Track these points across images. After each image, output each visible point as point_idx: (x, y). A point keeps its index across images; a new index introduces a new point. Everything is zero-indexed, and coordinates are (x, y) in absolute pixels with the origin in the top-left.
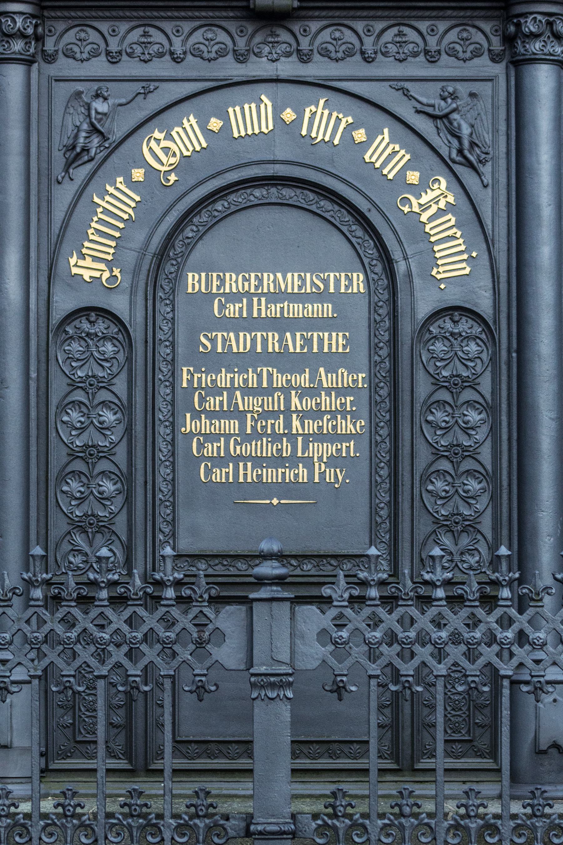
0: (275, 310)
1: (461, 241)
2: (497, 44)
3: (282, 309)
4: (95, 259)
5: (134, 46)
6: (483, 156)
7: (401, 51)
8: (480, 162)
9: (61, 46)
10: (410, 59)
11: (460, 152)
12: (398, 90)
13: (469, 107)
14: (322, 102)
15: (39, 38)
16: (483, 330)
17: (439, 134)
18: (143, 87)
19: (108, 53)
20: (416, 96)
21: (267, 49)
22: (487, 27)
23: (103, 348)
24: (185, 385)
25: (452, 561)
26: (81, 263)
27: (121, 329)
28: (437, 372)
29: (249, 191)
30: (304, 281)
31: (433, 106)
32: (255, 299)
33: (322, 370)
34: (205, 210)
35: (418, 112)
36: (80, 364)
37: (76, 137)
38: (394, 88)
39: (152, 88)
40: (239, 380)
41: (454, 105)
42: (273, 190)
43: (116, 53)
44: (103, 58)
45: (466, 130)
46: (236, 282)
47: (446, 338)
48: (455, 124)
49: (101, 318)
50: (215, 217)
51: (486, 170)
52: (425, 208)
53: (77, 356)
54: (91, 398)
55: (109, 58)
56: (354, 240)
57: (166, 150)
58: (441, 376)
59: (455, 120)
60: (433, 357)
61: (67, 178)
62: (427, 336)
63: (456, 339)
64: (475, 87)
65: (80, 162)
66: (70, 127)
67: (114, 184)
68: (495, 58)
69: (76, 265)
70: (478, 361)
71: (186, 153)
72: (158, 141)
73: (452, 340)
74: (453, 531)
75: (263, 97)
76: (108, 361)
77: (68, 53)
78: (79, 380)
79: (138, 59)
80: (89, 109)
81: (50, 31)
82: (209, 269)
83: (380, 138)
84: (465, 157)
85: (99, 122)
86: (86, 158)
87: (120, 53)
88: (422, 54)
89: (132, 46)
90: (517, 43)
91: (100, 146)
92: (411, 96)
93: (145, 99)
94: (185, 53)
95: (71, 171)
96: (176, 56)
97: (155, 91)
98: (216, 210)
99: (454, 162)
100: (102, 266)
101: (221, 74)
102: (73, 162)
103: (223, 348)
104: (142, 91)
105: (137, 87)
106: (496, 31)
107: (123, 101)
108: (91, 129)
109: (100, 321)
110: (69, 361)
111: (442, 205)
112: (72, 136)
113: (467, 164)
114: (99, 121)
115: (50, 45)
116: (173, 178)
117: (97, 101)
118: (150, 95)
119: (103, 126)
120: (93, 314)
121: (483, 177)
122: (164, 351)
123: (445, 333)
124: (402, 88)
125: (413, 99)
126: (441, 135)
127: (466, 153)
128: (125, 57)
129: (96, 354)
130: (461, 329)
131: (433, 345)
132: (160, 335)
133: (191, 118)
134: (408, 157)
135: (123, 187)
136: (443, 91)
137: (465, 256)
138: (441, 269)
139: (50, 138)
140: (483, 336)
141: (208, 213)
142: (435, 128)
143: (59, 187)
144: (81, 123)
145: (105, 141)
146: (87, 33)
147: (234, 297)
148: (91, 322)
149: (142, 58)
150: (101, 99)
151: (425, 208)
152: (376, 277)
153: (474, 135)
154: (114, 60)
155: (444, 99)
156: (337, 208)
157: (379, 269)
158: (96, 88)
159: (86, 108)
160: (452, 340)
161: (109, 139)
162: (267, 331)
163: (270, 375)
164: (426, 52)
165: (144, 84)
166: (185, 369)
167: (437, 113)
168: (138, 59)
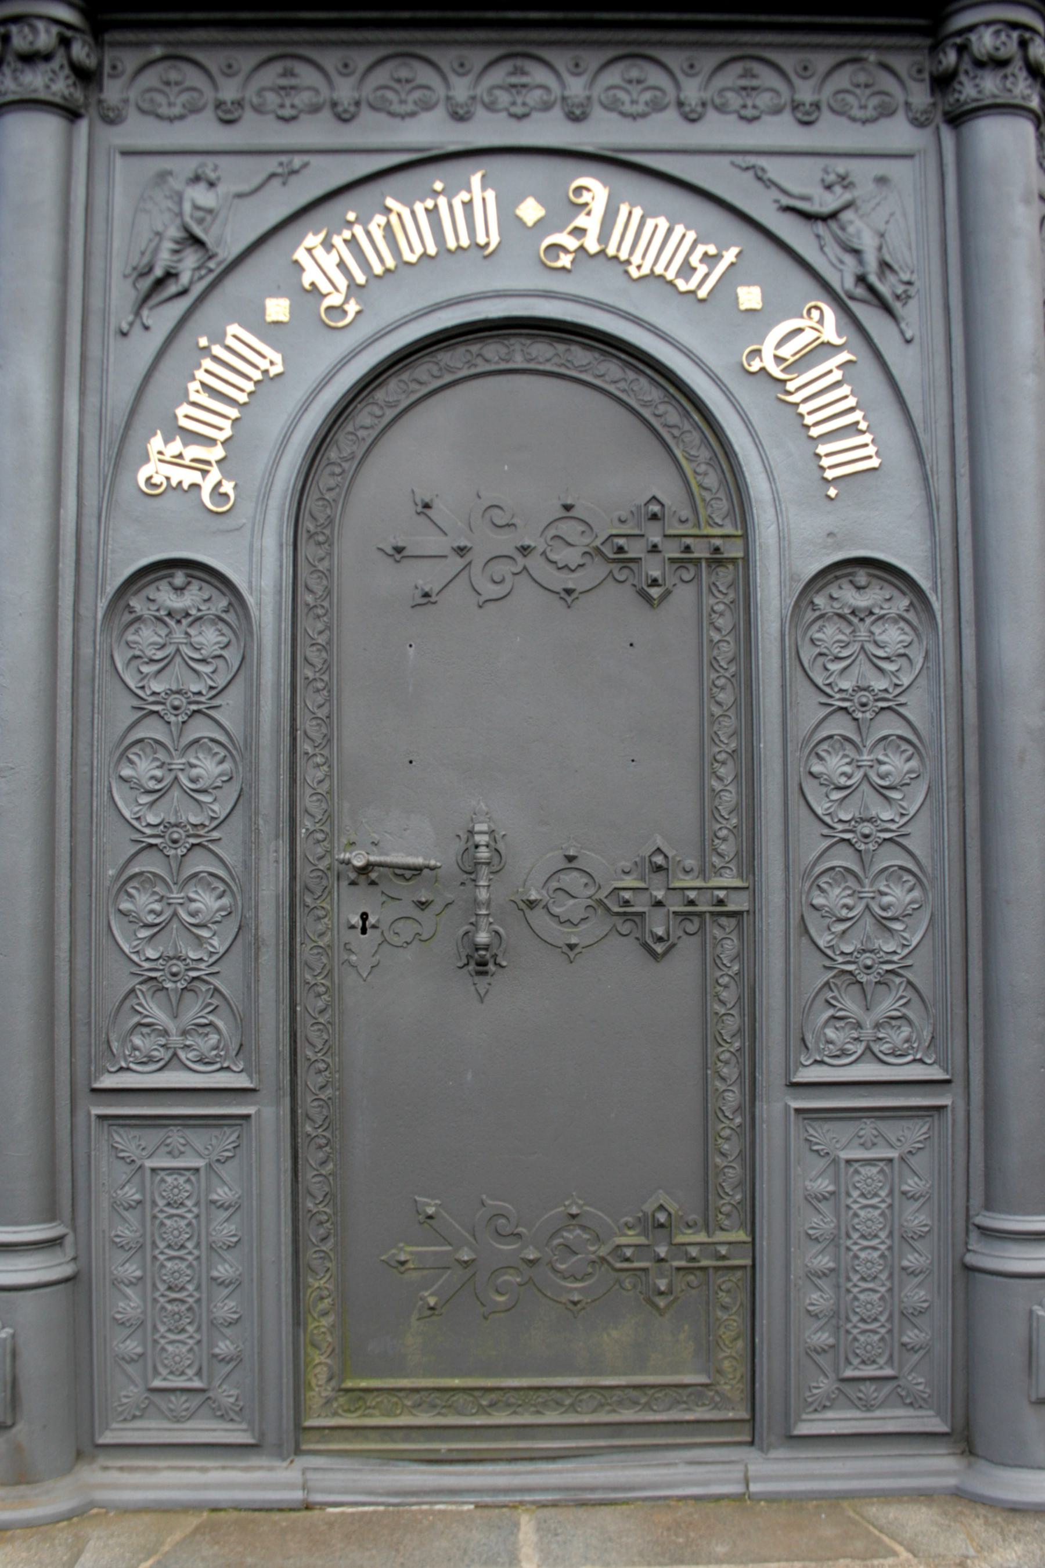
1: (867, 438)
2: (921, 96)
7: (749, 103)
8: (898, 297)
11: (861, 279)
12: (747, 169)
13: (877, 200)
16: (912, 604)
17: (822, 248)
19: (219, 105)
22: (901, 63)
23: (200, 639)
25: (857, 1039)
36: (156, 667)
37: (156, 251)
41: (847, 196)
44: (209, 113)
48: (851, 229)
51: (909, 312)
53: (150, 652)
54: (175, 733)
58: (836, 689)
59: (851, 222)
60: (821, 654)
61: (137, 329)
63: (862, 620)
70: (903, 661)
73: (855, 620)
74: (861, 983)
76: (208, 663)
77: (146, 106)
78: (151, 699)
80: (180, 202)
84: (871, 289)
87: (239, 104)
88: (788, 109)
91: (199, 268)
92: (770, 180)
94: (357, 104)
95: (145, 313)
99: (852, 298)
102: (147, 297)
104: (280, 170)
105: (271, 164)
106: (920, 71)
107: (245, 188)
109: (195, 585)
113: (875, 301)
114: (200, 221)
118: (293, 179)
119: (206, 231)
121: (903, 326)
126: (826, 249)
127: (873, 279)
128: (249, 115)
129: (186, 650)
140: (911, 616)
143: (126, 342)
144: (166, 226)
145: (210, 258)
153: (884, 250)
155: (829, 187)
164: (796, 106)
165: (284, 159)
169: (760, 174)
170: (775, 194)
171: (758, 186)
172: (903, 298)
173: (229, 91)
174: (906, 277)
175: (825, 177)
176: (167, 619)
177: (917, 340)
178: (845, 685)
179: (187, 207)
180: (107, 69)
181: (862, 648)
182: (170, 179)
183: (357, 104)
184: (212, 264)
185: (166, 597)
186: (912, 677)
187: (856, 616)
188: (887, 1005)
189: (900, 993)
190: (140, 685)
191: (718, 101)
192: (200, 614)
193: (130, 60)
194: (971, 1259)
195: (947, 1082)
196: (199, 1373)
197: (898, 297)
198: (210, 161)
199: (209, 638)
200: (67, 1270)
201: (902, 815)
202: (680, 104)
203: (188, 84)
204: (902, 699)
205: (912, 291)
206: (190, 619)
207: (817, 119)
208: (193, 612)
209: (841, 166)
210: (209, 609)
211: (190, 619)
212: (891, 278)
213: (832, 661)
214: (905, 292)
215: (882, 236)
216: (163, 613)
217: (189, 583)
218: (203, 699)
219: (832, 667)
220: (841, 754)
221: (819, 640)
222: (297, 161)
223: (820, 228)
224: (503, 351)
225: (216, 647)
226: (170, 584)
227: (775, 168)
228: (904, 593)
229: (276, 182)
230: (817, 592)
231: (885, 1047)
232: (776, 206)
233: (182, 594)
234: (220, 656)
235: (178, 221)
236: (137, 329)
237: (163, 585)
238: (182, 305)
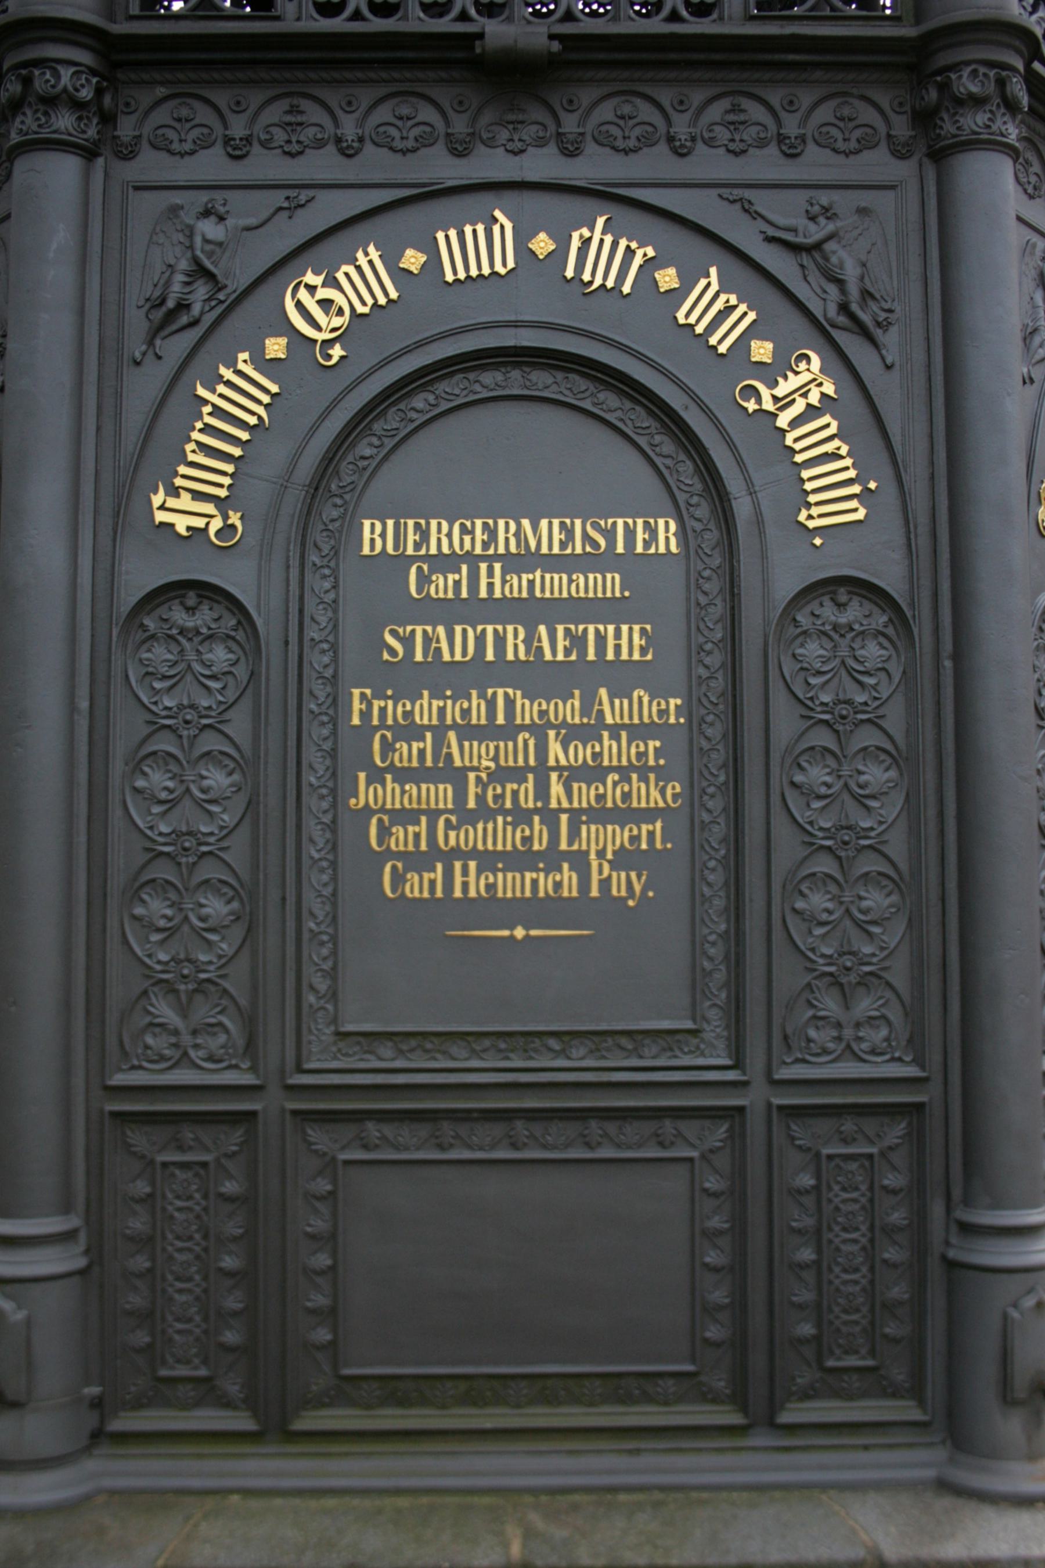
0: (518, 585)
1: (848, 462)
2: (902, 128)
3: (531, 583)
4: (197, 496)
5: (275, 130)
6: (884, 315)
7: (737, 137)
8: (879, 324)
9: (147, 130)
10: (752, 150)
11: (844, 308)
12: (734, 201)
13: (859, 231)
14: (600, 222)
15: (108, 119)
16: (890, 620)
18: (288, 198)
19: (228, 141)
20: (764, 212)
21: (504, 135)
23: (210, 656)
24: (356, 721)
26: (172, 503)
27: (242, 620)
28: (809, 695)
29: (472, 376)
30: (570, 533)
31: (794, 230)
32: (483, 566)
33: (603, 692)
34: (394, 409)
35: (771, 240)
37: (168, 284)
38: (727, 199)
39: (303, 198)
40: (453, 712)
41: (831, 227)
42: (516, 374)
43: (241, 139)
44: (218, 149)
45: (851, 273)
46: (449, 535)
47: (825, 633)
48: (834, 260)
49: (205, 601)
50: (412, 421)
51: (890, 339)
52: (784, 403)
53: (164, 670)
55: (229, 149)
56: (658, 461)
57: (325, 304)
58: (817, 703)
59: (834, 252)
60: (802, 669)
61: (150, 355)
62: (792, 631)
63: (842, 636)
64: (865, 198)
65: (174, 327)
66: (159, 267)
67: (232, 364)
68: (900, 153)
69: (162, 507)
70: (883, 675)
71: (361, 309)
72: (312, 289)
73: (836, 637)
75: (497, 214)
79: (279, 151)
80: (191, 236)
81: (127, 105)
82: (399, 514)
83: (703, 282)
85: (209, 258)
86: (184, 320)
87: (248, 140)
88: (774, 143)
89: (271, 129)
90: (942, 119)
91: (209, 299)
92: (756, 212)
93: (290, 217)
94: (361, 140)
95: (158, 342)
96: (345, 145)
97: (309, 205)
98: (413, 409)
99: (834, 326)
100: (209, 508)
101: (423, 177)
102: (162, 326)
103: (425, 654)
104: (286, 205)
105: (278, 198)
106: (901, 104)
107: (253, 221)
108: (194, 268)
111: (814, 398)
112: (162, 282)
113: (856, 329)
114: (210, 255)
115: (126, 129)
116: (337, 352)
117: (206, 221)
118: (300, 212)
120: (192, 594)
121: (884, 352)
122: (318, 660)
123: (823, 624)
124: (741, 199)
125: (759, 219)
126: (809, 278)
127: (854, 307)
128: (256, 149)
130: (851, 618)
131: (802, 645)
132: (312, 633)
133: (371, 249)
134: (752, 316)
135: (248, 370)
136: (812, 205)
137: (856, 489)
138: (815, 511)
139: (122, 288)
140: (890, 631)
141: (399, 413)
142: (798, 267)
145: (220, 290)
146: (192, 108)
147: (445, 563)
148: (188, 609)
149: (286, 149)
150: (213, 219)
151: (784, 403)
152: (698, 526)
154: (238, 153)
155: (813, 219)
156: (628, 405)
157: (703, 511)
158: (205, 199)
159: (188, 233)
160: (836, 637)
161: (226, 286)
162: (504, 623)
163: (510, 703)
164: (781, 139)
165: (292, 193)
166: (356, 692)
167: (800, 240)
168: (279, 151)
169: (747, 207)
171: (745, 217)
173: (238, 129)
175: (809, 208)
176: (180, 638)
177: (897, 367)
178: (826, 698)
179: (198, 240)
180: (121, 107)
181: (843, 662)
182: (182, 213)
183: (361, 140)
184: (221, 296)
185: (179, 616)
186: (890, 692)
187: (836, 632)
188: (865, 1005)
189: (879, 994)
191: (706, 135)
193: (145, 98)
194: (952, 1254)
195: (926, 1080)
196: (205, 1362)
197: (879, 324)
198: (218, 195)
199: (220, 655)
201: (881, 823)
202: (670, 139)
203: (197, 121)
204: (880, 712)
205: (893, 317)
207: (802, 151)
209: (824, 198)
212: (873, 306)
213: (814, 675)
214: (886, 319)
215: (864, 265)
217: (200, 603)
219: (813, 681)
220: (821, 765)
221: (801, 655)
222: (303, 197)
223: (806, 260)
224: (499, 376)
225: (225, 664)
226: (182, 604)
227: (761, 201)
228: (884, 611)
229: (285, 214)
230: (799, 610)
231: (864, 1046)
232: (762, 236)
234: (230, 673)
235: (189, 254)
236: (150, 355)
237: (176, 605)
238: (193, 335)
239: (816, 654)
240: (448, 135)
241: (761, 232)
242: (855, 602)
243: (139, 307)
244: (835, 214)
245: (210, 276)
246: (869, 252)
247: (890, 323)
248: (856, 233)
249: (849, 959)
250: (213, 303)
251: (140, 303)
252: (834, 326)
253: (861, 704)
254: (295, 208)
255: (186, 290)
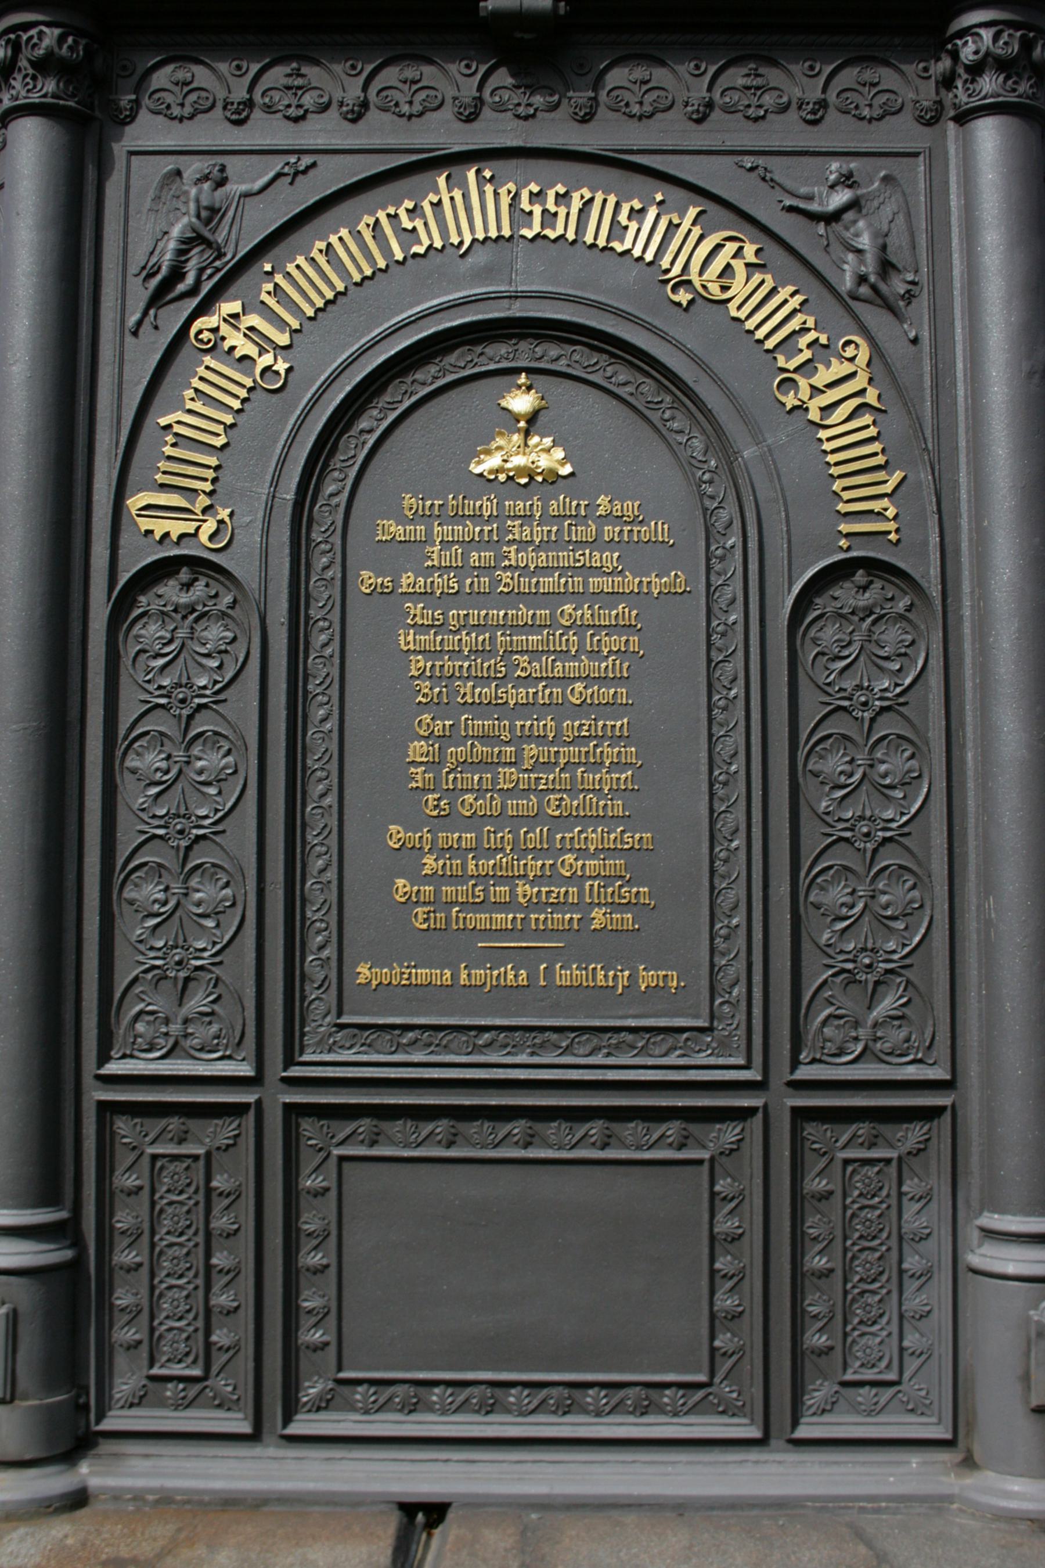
2: (928, 92)
11: (862, 279)
13: (881, 199)
31: (810, 198)
36: (161, 662)
78: (157, 693)
84: (874, 288)
86: (181, 287)
92: (772, 180)
93: (291, 184)
95: (152, 312)
105: (277, 164)
109: (200, 585)
110: (143, 657)
113: (879, 301)
118: (300, 178)
119: (214, 231)
124: (757, 167)
125: (777, 187)
127: (872, 279)
161: (225, 254)
165: (293, 159)
170: (778, 194)
172: (909, 297)
174: (910, 277)
184: (217, 263)
190: (147, 678)
192: (207, 609)
200: (68, 1254)
206: (196, 614)
207: (822, 118)
208: (200, 608)
210: (215, 605)
211: (196, 614)
214: (908, 292)
216: (170, 608)
218: (208, 692)
222: (306, 160)
223: (821, 228)
233: (188, 591)
236: (146, 326)
239: (836, 638)
240: (455, 99)
241: (781, 201)
242: (878, 584)
243: (136, 276)
244: (855, 182)
245: (209, 244)
246: (891, 222)
247: (914, 296)
248: (876, 203)
249: (865, 957)
250: (209, 271)
251: (136, 272)
252: (855, 298)
253: (882, 690)
254: (297, 173)
255: (183, 258)
